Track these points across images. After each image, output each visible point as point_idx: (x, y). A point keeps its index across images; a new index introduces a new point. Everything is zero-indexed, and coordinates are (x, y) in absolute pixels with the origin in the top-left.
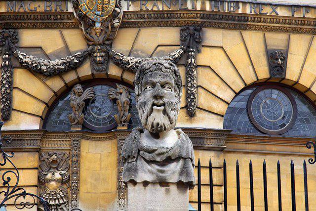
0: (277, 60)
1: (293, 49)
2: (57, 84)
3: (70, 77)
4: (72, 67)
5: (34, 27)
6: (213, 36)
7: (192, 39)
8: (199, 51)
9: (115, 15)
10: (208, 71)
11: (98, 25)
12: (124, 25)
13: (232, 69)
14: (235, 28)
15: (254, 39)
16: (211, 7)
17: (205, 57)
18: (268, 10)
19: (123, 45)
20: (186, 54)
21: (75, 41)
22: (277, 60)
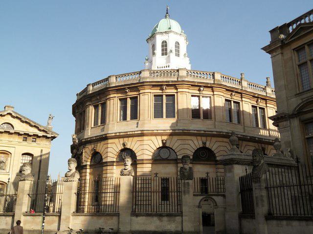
18: (92, 138)
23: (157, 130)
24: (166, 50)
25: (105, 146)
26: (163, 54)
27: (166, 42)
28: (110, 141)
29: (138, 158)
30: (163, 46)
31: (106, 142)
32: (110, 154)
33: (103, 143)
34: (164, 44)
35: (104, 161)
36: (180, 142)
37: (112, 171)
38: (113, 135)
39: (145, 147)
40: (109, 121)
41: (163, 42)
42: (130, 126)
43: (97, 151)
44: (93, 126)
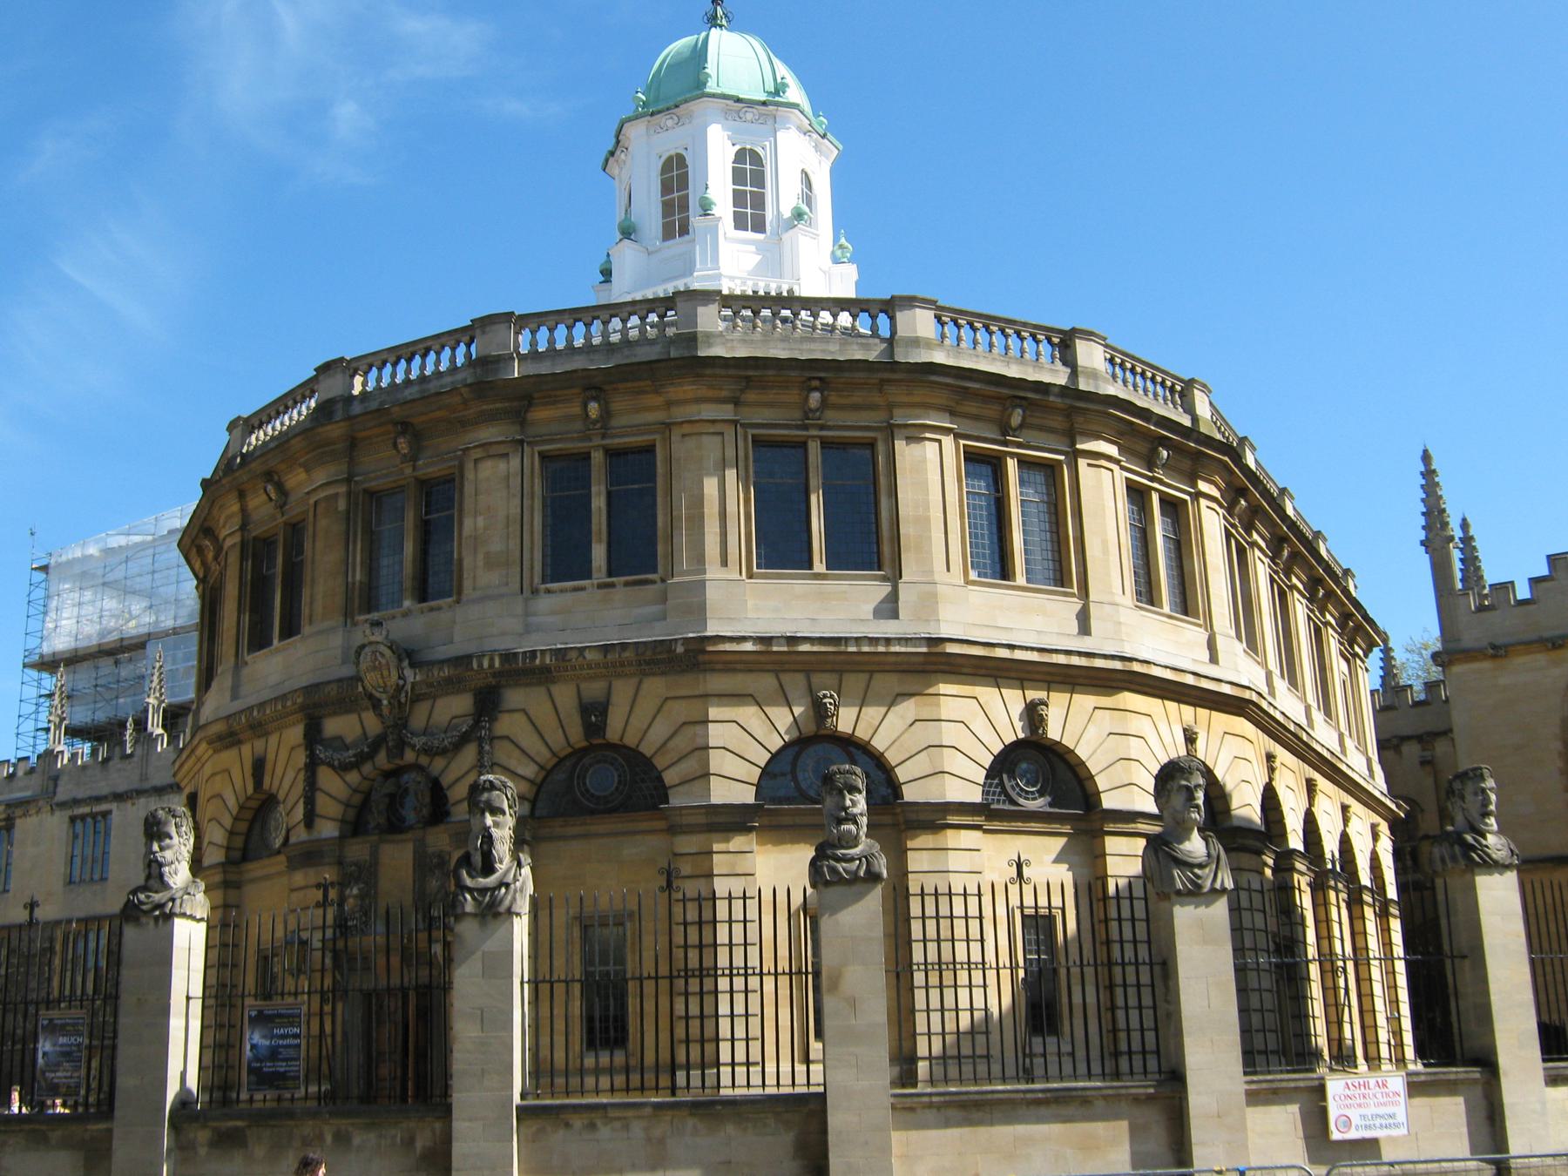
0: (594, 714)
1: (614, 699)
2: (353, 777)
3: (367, 768)
4: (361, 759)
5: (335, 714)
6: (514, 697)
7: (488, 703)
8: (493, 719)
9: (399, 689)
10: (506, 744)
11: (385, 702)
12: (416, 699)
13: (535, 738)
14: (539, 683)
15: (565, 695)
16: (501, 663)
17: (506, 724)
19: (418, 719)
20: (477, 724)
21: (373, 724)
22: (594, 714)
23: (1011, 647)
24: (759, 202)
25: (680, 711)
26: (740, 222)
27: (756, 159)
28: (717, 682)
29: (910, 794)
30: (738, 176)
31: (686, 684)
32: (719, 762)
33: (655, 687)
34: (750, 170)
35: (677, 800)
36: (1105, 721)
37: (743, 864)
38: (748, 646)
39: (949, 734)
40: (700, 559)
41: (740, 156)
42: (824, 606)
43: (613, 732)
44: (537, 579)
